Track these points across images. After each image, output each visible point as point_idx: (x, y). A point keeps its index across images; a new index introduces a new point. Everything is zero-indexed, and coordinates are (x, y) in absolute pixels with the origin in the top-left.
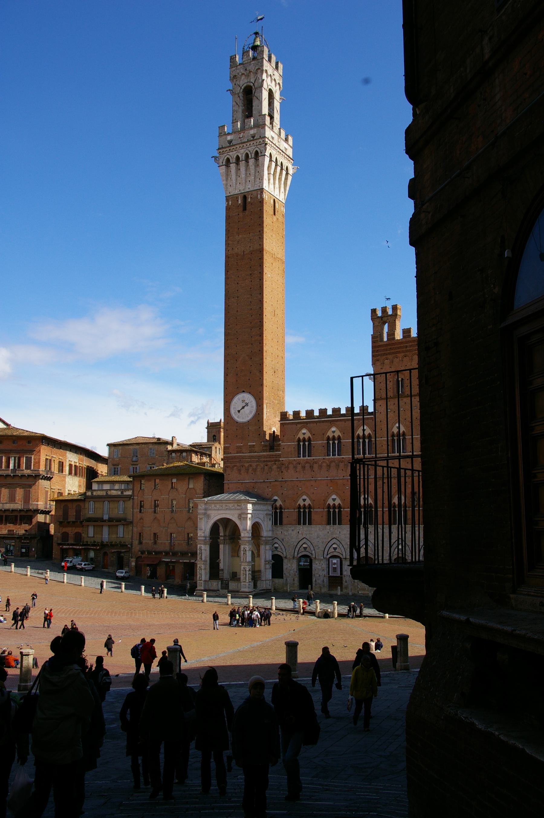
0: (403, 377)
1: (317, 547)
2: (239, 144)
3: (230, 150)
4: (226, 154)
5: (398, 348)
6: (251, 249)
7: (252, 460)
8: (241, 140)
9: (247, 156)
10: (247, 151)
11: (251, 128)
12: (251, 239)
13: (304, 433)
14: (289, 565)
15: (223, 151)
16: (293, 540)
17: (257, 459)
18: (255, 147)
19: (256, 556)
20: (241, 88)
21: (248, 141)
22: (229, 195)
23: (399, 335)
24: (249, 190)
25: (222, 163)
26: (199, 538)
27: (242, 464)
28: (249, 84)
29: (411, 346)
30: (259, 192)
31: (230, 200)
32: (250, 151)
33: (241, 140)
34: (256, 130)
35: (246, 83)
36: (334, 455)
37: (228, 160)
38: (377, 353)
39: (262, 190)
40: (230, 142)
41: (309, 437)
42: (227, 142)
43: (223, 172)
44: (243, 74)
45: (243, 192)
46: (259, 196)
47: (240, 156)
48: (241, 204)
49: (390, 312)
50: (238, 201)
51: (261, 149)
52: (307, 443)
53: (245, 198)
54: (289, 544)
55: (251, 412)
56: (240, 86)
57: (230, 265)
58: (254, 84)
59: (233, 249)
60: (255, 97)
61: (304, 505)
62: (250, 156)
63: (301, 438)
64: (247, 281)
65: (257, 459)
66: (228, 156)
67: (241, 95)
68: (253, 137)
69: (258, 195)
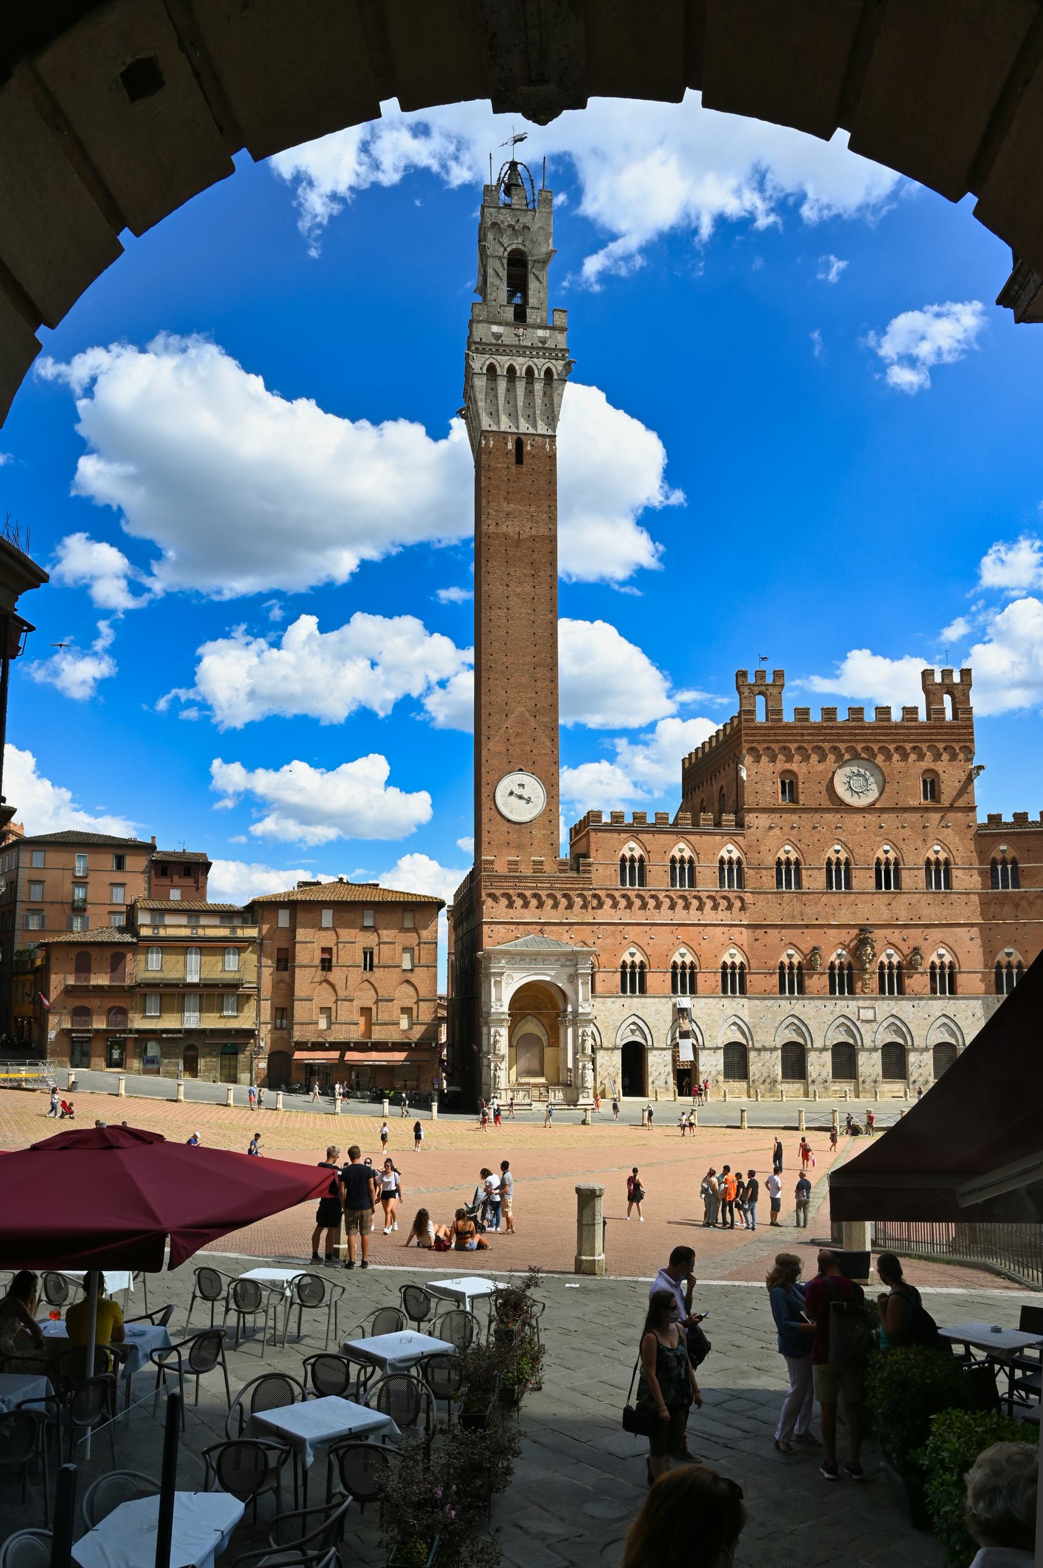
0: (792, 779)
1: (656, 1029)
2: (516, 346)
4: (488, 356)
5: (789, 735)
6: (534, 532)
7: (539, 885)
8: (519, 340)
9: (530, 371)
10: (530, 363)
11: (540, 327)
13: (632, 848)
14: (607, 1058)
16: (614, 1018)
17: (548, 885)
19: (545, 1043)
20: (505, 249)
21: (532, 347)
22: (489, 429)
23: (788, 717)
24: (528, 432)
26: (493, 1017)
27: (520, 891)
28: (520, 246)
29: (810, 734)
33: (519, 340)
34: (548, 331)
36: (632, 884)
37: (491, 368)
38: (752, 738)
39: (553, 437)
40: (497, 336)
41: (641, 855)
42: (490, 334)
44: (510, 226)
45: (516, 431)
46: (547, 446)
47: (517, 367)
48: (514, 451)
49: (769, 680)
50: (506, 444)
52: (637, 865)
53: (519, 444)
54: (607, 1025)
55: (536, 806)
57: (491, 551)
59: (497, 524)
61: (633, 962)
62: (536, 372)
63: (628, 855)
64: (525, 584)
65: (548, 885)
66: (491, 360)
67: (505, 261)
68: (544, 343)
69: (545, 444)
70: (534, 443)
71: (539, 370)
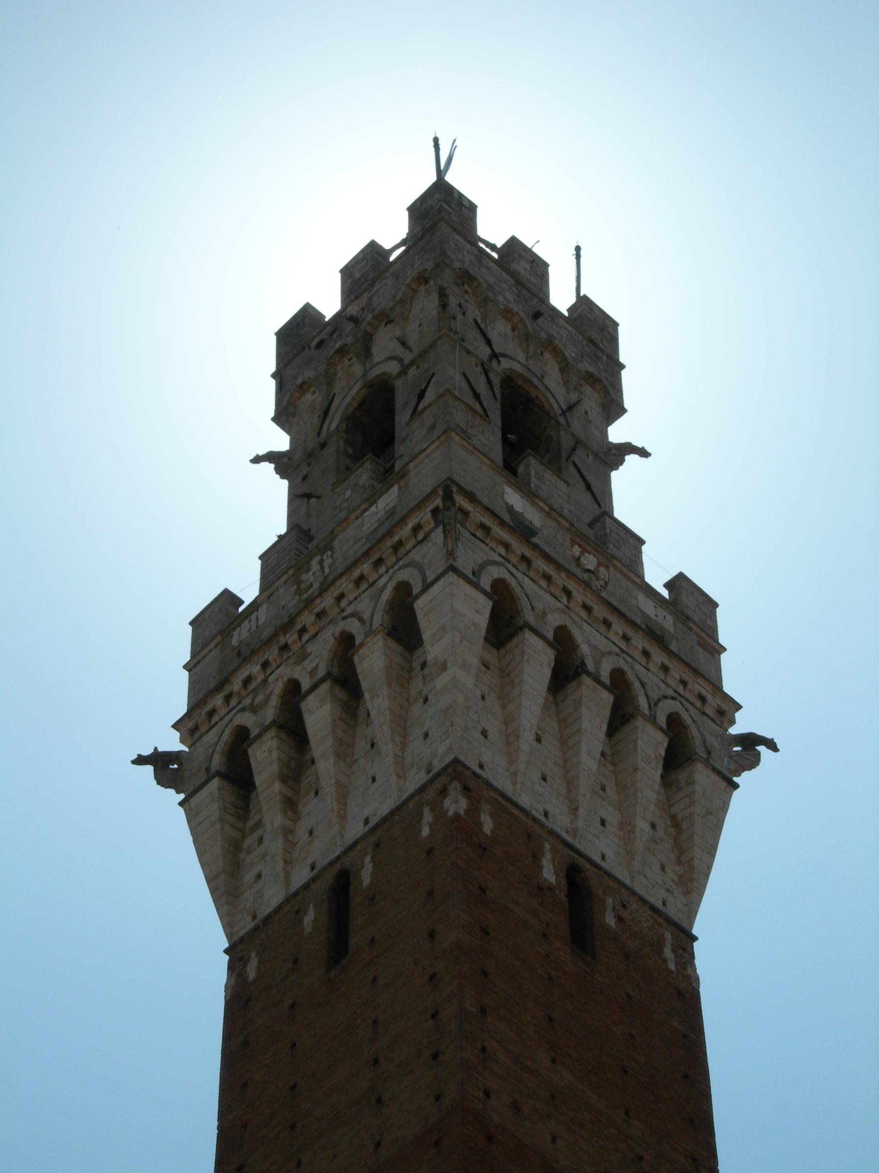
3: (524, 558)
12: (640, 1158)
15: (482, 526)
18: (670, 693)
25: (474, 574)
28: (536, 381)
30: (668, 935)
31: (486, 808)
32: (643, 685)
35: (519, 362)
43: (475, 624)
46: (668, 953)
47: (585, 649)
50: (537, 857)
51: (709, 738)
56: (489, 342)
58: (564, 413)
60: (572, 469)
62: (643, 702)
70: (625, 915)
71: (654, 705)
